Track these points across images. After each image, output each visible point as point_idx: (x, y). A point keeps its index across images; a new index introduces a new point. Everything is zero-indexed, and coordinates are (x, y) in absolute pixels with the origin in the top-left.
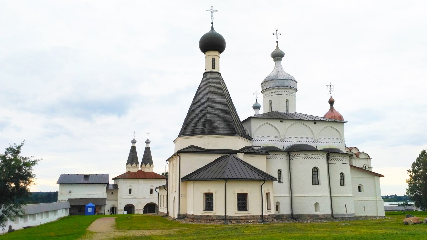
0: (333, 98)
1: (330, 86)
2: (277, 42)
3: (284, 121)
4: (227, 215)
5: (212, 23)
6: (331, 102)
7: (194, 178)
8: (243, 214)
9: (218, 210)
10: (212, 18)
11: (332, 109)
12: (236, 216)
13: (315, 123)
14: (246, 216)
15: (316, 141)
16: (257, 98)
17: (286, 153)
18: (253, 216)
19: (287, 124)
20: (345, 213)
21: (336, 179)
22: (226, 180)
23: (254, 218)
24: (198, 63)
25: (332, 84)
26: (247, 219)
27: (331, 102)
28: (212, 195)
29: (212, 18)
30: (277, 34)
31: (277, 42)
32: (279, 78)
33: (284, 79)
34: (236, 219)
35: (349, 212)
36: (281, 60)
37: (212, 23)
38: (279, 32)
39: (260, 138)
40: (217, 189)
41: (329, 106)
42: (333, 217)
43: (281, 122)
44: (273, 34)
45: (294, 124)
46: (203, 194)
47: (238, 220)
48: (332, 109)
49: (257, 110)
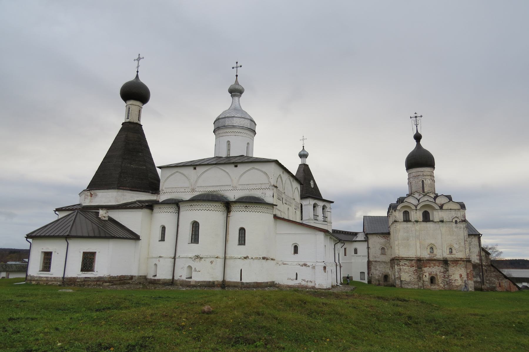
0: (419, 132)
1: (416, 117)
2: (237, 76)
3: (197, 168)
5: (138, 72)
6: (418, 137)
8: (45, 275)
9: (56, 271)
10: (138, 67)
11: (419, 146)
12: (37, 277)
13: (236, 166)
14: (47, 277)
15: (235, 188)
17: (174, 206)
18: (54, 278)
21: (234, 235)
25: (419, 115)
26: (47, 280)
27: (418, 137)
29: (138, 67)
30: (237, 66)
31: (237, 76)
33: (225, 118)
34: (37, 280)
37: (138, 72)
38: (239, 65)
39: (168, 190)
40: (56, 248)
41: (414, 143)
42: (172, 282)
43: (195, 169)
44: (233, 68)
45: (207, 170)
48: (419, 146)
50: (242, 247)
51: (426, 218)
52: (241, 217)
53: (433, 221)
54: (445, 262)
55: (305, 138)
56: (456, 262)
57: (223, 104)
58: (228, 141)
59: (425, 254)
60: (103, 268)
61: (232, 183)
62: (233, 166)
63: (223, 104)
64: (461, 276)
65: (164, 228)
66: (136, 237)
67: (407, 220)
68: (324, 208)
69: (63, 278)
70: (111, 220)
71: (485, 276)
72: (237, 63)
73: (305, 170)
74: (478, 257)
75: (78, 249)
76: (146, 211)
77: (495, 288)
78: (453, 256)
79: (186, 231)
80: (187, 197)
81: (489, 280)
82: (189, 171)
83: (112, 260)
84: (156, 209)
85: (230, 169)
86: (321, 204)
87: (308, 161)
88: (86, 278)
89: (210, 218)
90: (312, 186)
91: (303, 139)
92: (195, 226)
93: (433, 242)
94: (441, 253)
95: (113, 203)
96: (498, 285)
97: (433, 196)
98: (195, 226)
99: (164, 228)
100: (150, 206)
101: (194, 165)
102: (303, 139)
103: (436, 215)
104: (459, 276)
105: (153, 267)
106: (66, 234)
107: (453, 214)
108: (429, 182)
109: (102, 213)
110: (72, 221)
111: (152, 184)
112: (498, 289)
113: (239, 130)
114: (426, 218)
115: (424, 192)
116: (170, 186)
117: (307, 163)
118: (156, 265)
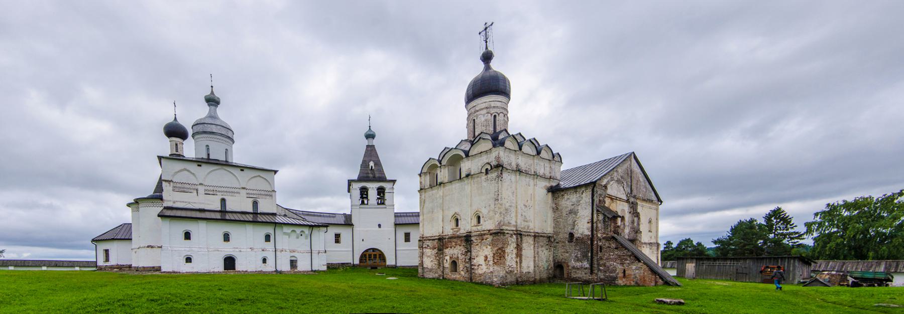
6: (487, 58)
27: (487, 58)
50: (188, 241)
54: (467, 239)
56: (481, 236)
59: (449, 231)
64: (486, 257)
68: (381, 191)
71: (595, 258)
74: (590, 225)
77: (615, 278)
78: (479, 228)
81: (604, 265)
86: (372, 187)
93: (457, 210)
94: (467, 226)
96: (621, 275)
104: (483, 258)
107: (484, 159)
108: (483, 119)
112: (620, 282)
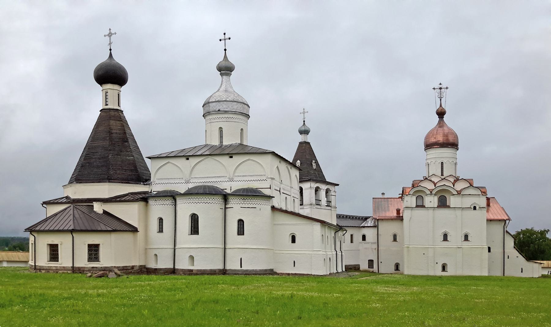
3: (190, 159)
4: (37, 264)
7: (37, 229)
8: (53, 264)
13: (231, 157)
16: (304, 118)
18: (64, 267)
19: (237, 160)
20: (239, 268)
22: (72, 231)
23: (64, 268)
24: (94, 100)
26: (57, 270)
28: (57, 246)
32: (210, 101)
35: (244, 268)
36: (229, 75)
46: (46, 245)
47: (48, 270)
49: (303, 136)
51: (443, 204)
52: (237, 209)
53: (449, 207)
55: (306, 111)
57: (213, 86)
58: (221, 128)
60: (106, 260)
61: (228, 174)
62: (227, 158)
63: (213, 86)
65: (161, 220)
66: (134, 230)
67: (420, 206)
69: (73, 267)
70: (105, 212)
72: (225, 34)
73: (305, 152)
75: (84, 241)
76: (142, 204)
79: (184, 224)
80: (182, 189)
82: (181, 162)
83: (115, 252)
84: (151, 202)
85: (225, 160)
87: (309, 138)
88: (93, 267)
89: (208, 210)
90: (314, 167)
91: (304, 113)
92: (194, 219)
95: (106, 196)
97: (452, 180)
98: (194, 219)
99: (161, 220)
100: (144, 198)
101: (185, 155)
102: (304, 113)
103: (453, 201)
105: (153, 258)
106: (71, 228)
109: (98, 208)
110: (72, 216)
111: (140, 175)
113: (231, 116)
114: (443, 204)
115: (442, 175)
116: (163, 177)
117: (308, 141)
118: (156, 255)
